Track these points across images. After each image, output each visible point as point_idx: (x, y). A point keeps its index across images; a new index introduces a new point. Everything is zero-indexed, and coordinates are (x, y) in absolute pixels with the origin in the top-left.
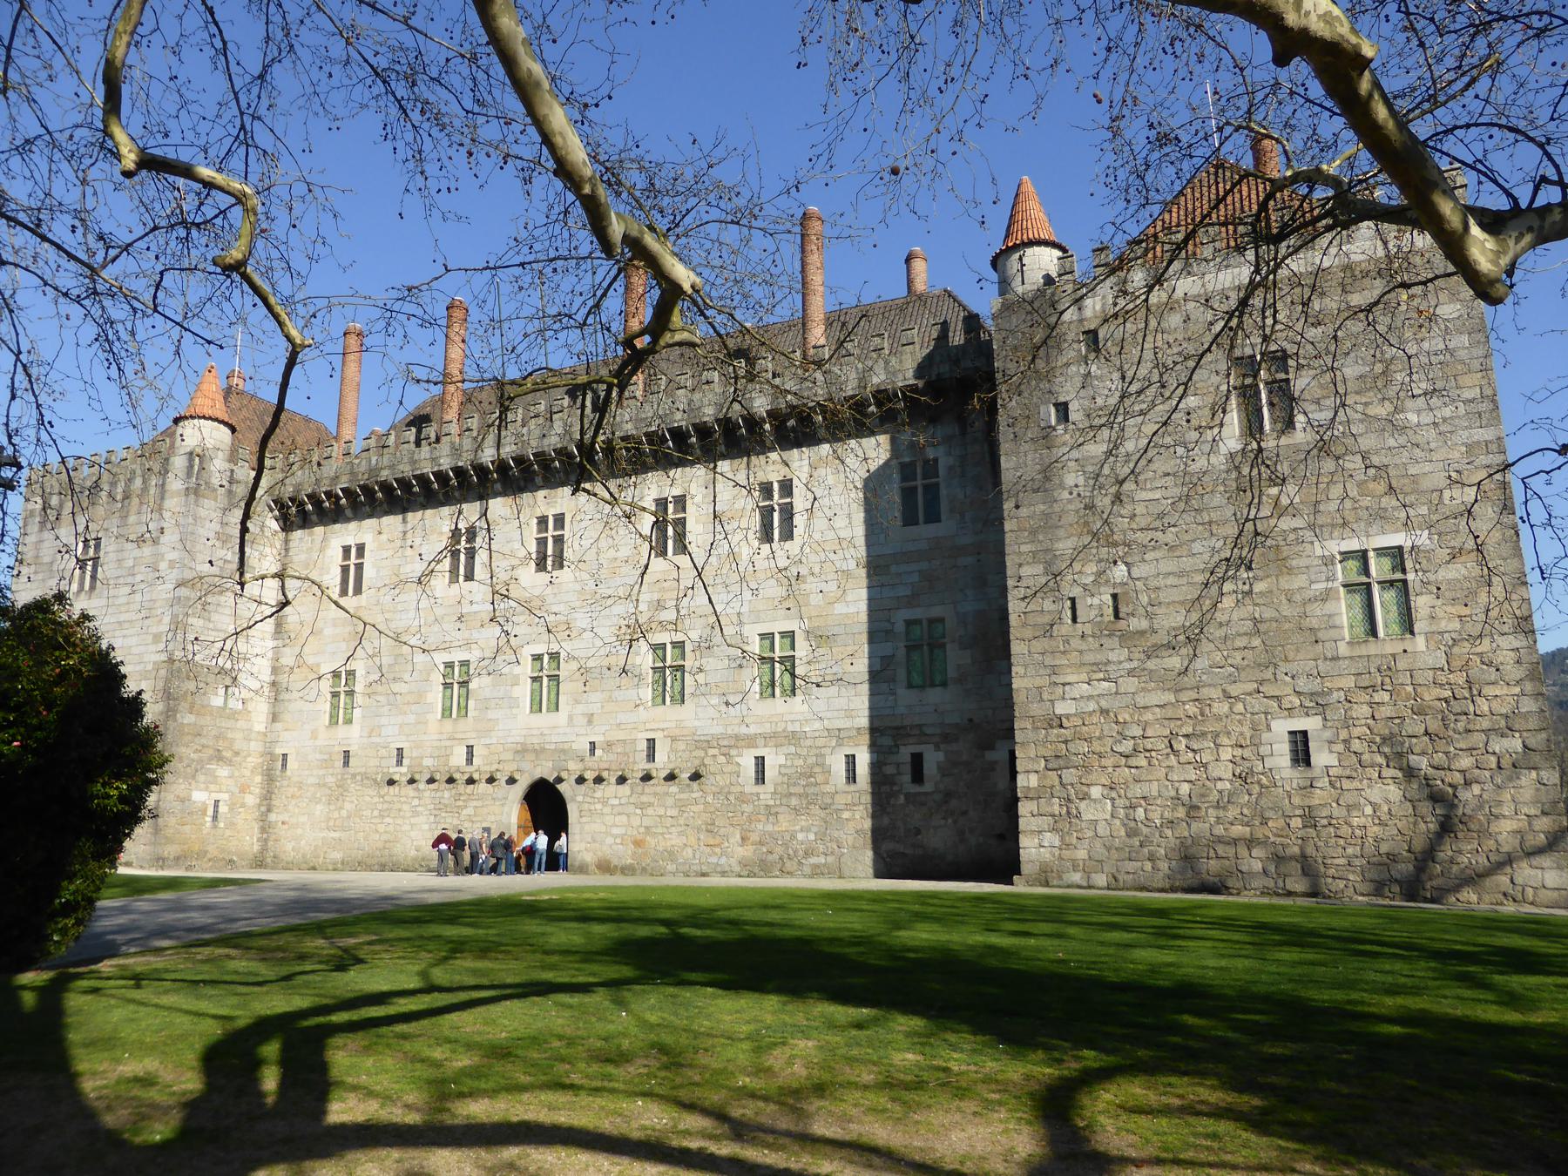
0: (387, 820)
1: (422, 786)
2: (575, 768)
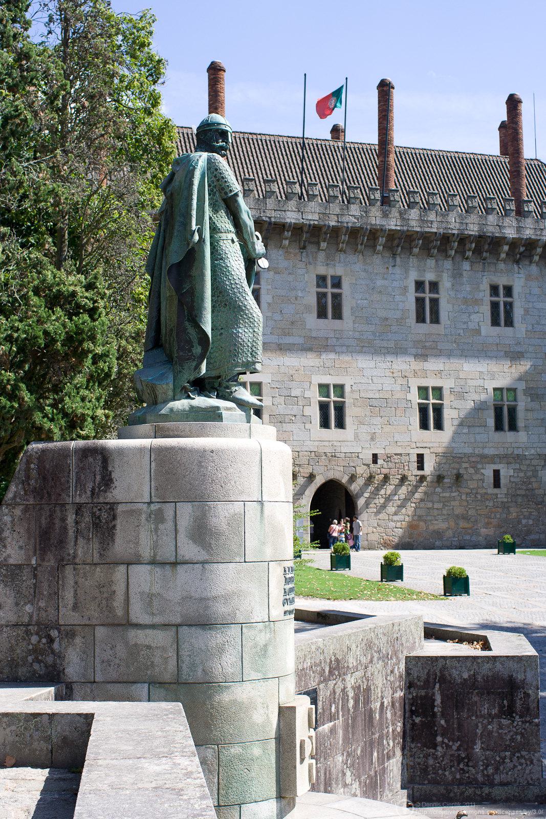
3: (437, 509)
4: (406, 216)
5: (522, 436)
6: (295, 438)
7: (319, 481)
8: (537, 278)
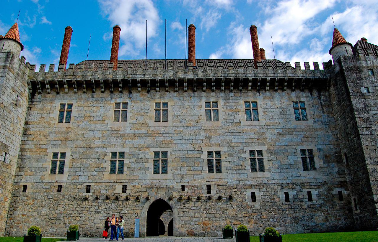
0: (81, 215)
1: (100, 201)
2: (175, 195)
3: (219, 214)
4: (196, 73)
5: (267, 174)
6: (140, 179)
7: (152, 200)
8: (269, 98)
